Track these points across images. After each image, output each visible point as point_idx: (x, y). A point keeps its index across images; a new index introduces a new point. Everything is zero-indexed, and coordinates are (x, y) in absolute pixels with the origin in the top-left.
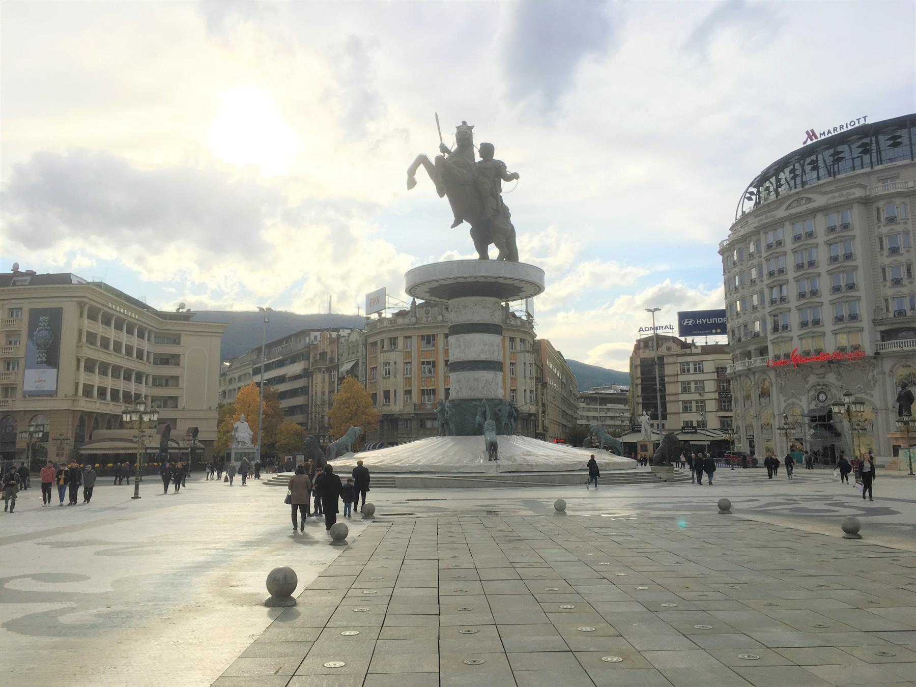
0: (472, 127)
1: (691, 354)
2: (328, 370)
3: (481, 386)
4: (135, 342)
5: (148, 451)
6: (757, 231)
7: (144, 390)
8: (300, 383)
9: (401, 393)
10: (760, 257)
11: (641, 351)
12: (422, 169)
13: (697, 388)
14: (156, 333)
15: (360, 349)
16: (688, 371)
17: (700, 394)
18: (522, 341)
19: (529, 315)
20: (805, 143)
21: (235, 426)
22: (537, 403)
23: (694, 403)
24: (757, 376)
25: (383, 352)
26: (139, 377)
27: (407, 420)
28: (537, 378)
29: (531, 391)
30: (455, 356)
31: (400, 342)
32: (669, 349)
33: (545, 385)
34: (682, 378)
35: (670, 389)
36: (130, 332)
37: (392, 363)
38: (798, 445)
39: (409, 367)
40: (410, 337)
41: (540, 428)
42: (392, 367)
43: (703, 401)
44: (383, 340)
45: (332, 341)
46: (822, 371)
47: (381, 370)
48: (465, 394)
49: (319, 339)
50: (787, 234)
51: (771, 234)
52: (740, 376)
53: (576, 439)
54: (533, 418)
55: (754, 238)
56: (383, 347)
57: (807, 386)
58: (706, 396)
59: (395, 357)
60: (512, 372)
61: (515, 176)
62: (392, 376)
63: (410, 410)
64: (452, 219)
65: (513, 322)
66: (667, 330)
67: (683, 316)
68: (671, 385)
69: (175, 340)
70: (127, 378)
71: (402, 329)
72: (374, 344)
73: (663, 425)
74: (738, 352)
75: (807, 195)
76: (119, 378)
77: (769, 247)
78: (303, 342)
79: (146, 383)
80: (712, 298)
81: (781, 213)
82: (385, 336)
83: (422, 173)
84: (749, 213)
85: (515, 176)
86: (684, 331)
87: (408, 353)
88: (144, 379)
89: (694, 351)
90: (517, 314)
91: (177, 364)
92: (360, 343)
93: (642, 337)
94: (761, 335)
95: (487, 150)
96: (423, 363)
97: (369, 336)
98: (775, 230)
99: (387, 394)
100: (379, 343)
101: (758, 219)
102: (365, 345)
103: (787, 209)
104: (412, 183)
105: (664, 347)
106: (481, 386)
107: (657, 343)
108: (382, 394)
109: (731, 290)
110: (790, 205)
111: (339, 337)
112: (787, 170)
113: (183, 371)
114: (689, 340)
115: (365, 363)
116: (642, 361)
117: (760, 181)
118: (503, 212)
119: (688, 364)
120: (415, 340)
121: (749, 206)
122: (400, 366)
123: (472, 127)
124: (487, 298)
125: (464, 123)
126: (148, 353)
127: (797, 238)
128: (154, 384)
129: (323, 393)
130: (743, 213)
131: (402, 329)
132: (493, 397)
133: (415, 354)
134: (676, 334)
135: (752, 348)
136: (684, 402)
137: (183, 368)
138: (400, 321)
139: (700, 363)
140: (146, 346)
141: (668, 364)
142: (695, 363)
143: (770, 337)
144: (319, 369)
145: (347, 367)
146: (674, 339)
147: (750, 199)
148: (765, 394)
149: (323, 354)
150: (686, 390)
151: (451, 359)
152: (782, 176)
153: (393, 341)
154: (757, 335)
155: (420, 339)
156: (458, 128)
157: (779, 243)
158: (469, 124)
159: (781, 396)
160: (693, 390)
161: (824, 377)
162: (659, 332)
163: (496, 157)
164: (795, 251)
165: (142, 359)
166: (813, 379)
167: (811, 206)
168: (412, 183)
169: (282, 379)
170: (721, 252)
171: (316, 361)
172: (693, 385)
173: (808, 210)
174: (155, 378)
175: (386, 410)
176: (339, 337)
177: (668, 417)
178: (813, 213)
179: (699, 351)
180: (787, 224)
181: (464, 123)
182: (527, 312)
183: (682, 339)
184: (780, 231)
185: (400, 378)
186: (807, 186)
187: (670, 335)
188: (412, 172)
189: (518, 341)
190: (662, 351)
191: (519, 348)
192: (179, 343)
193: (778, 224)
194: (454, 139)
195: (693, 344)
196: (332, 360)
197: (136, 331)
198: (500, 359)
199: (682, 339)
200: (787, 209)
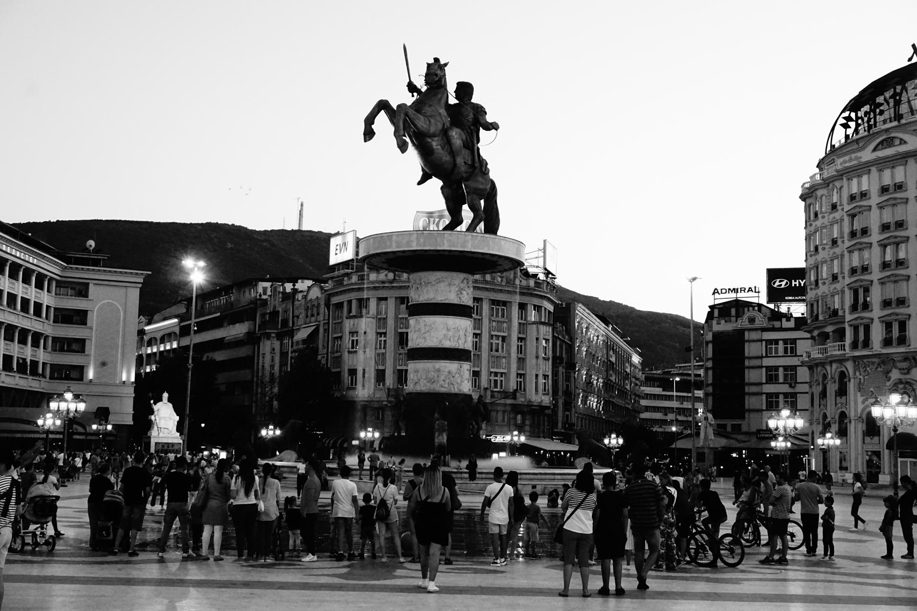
0: (446, 65)
1: (781, 329)
2: (280, 337)
3: (443, 378)
4: (32, 293)
5: (51, 436)
6: (840, 175)
7: (42, 356)
8: (243, 352)
9: (371, 374)
10: (843, 209)
11: (714, 322)
12: (382, 117)
13: (785, 376)
14: (57, 281)
16: (776, 352)
17: (791, 386)
18: (538, 308)
19: (548, 273)
20: (910, 60)
21: (155, 407)
23: (781, 397)
24: (834, 366)
25: (349, 317)
26: (37, 337)
27: (378, 409)
28: (555, 358)
29: (545, 377)
30: (416, 341)
31: (373, 304)
32: (752, 320)
34: (767, 362)
35: (752, 376)
36: (26, 281)
37: (361, 332)
38: (875, 458)
39: (383, 339)
40: (386, 299)
41: (560, 425)
42: (361, 338)
43: (794, 395)
44: (350, 302)
45: (290, 297)
46: (905, 365)
47: (347, 341)
48: (423, 387)
49: (269, 293)
50: (868, 183)
51: (855, 181)
52: (831, 363)
53: (566, 439)
54: (547, 412)
55: (838, 184)
56: (350, 311)
57: (888, 384)
58: (799, 388)
59: (366, 325)
60: (520, 350)
61: (494, 126)
62: (361, 352)
63: (381, 395)
64: (419, 175)
65: (524, 283)
66: (751, 294)
67: (773, 274)
68: (751, 370)
69: (82, 291)
70: (23, 341)
71: (375, 288)
72: (339, 306)
73: (740, 425)
74: (816, 333)
75: (900, 135)
76: (12, 340)
77: (852, 198)
78: (247, 294)
79: (45, 348)
80: (794, 257)
81: (867, 155)
82: (353, 296)
83: (382, 122)
84: (841, 147)
85: (494, 126)
86: (775, 295)
87: (381, 321)
88: (42, 341)
89: (785, 324)
90: (531, 270)
91: (86, 324)
92: (322, 303)
93: (717, 302)
94: (840, 313)
95: (465, 89)
98: (860, 176)
100: (345, 304)
101: (841, 160)
102: (327, 305)
103: (875, 150)
104: (369, 134)
105: (746, 317)
106: (443, 378)
107: (737, 312)
108: (346, 375)
109: (813, 250)
110: (881, 143)
111: (295, 291)
112: (888, 94)
113: (92, 333)
114: (783, 308)
115: (326, 331)
116: (717, 336)
117: (854, 105)
118: (479, 167)
119: (776, 342)
120: (391, 303)
121: (839, 137)
122: (371, 336)
123: (446, 65)
124: (454, 274)
125: (437, 60)
126: (48, 307)
127: (884, 190)
128: (54, 350)
129: (272, 367)
130: (833, 146)
131: (375, 288)
132: (456, 391)
133: (391, 322)
134: (763, 300)
135: (829, 329)
136: (769, 395)
137: (91, 328)
139: (794, 341)
140: (46, 299)
141: (749, 341)
142: (785, 341)
143: (848, 317)
144: (268, 336)
145: (302, 334)
146: (760, 306)
147: (846, 126)
148: (842, 391)
149: (275, 313)
150: (772, 378)
151: (411, 345)
152: (880, 99)
153: (363, 303)
154: (835, 313)
155: (399, 302)
156: (429, 65)
157: (864, 195)
158: (442, 62)
159: (859, 394)
160: (781, 380)
161: (908, 373)
162: (742, 296)
163: (474, 100)
164: (881, 207)
165: (40, 316)
166: (895, 375)
167: (903, 149)
168: (369, 134)
169: (219, 344)
170: (803, 197)
171: (263, 325)
172: (781, 369)
173: (899, 154)
174: (55, 339)
176: (295, 291)
177: (747, 415)
178: (904, 158)
179: (792, 324)
180: (874, 169)
181: (437, 60)
182: (546, 269)
183: (772, 306)
184: (865, 178)
185: (370, 353)
186: (903, 121)
187: (755, 300)
188: (370, 121)
189: (530, 308)
190: (743, 323)
192: (86, 295)
193: (862, 169)
194: (423, 82)
195: (788, 316)
196: (285, 322)
197: (34, 279)
198: (469, 346)
199: (772, 306)
200: (875, 150)
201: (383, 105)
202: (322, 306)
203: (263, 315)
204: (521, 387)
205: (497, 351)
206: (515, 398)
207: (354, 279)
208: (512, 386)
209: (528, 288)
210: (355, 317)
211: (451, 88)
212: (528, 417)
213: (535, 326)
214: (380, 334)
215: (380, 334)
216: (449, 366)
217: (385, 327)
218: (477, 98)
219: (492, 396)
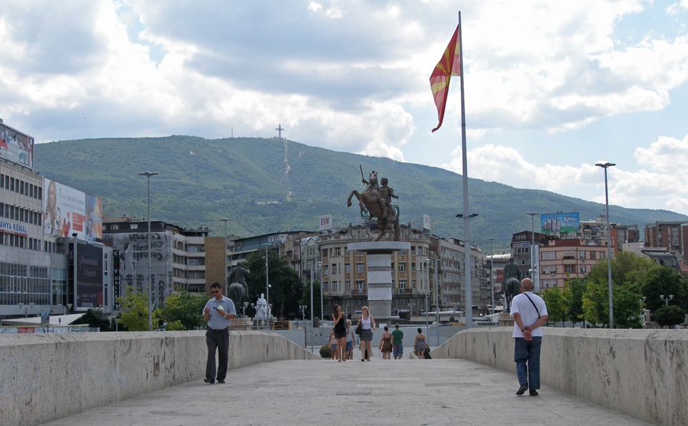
9: (343, 284)
12: (354, 198)
15: (316, 253)
18: (420, 247)
22: (431, 287)
33: (440, 272)
44: (331, 249)
59: (340, 261)
61: (397, 197)
63: (349, 294)
82: (332, 246)
95: (385, 182)
96: (357, 264)
97: (323, 245)
99: (335, 282)
100: (329, 250)
102: (319, 250)
104: (350, 204)
122: (343, 266)
138: (342, 237)
149: (289, 252)
168: (350, 204)
175: (334, 294)
185: (343, 275)
188: (349, 200)
189: (417, 248)
191: (417, 253)
196: (296, 257)
201: (355, 192)
202: (316, 249)
203: (282, 253)
204: (414, 286)
205: (402, 270)
206: (411, 292)
207: (333, 239)
208: (410, 286)
209: (416, 239)
210: (334, 257)
211: (379, 182)
212: (418, 300)
213: (419, 257)
214: (347, 264)
215: (347, 264)
216: (383, 290)
217: (349, 260)
218: (390, 185)
219: (401, 292)
